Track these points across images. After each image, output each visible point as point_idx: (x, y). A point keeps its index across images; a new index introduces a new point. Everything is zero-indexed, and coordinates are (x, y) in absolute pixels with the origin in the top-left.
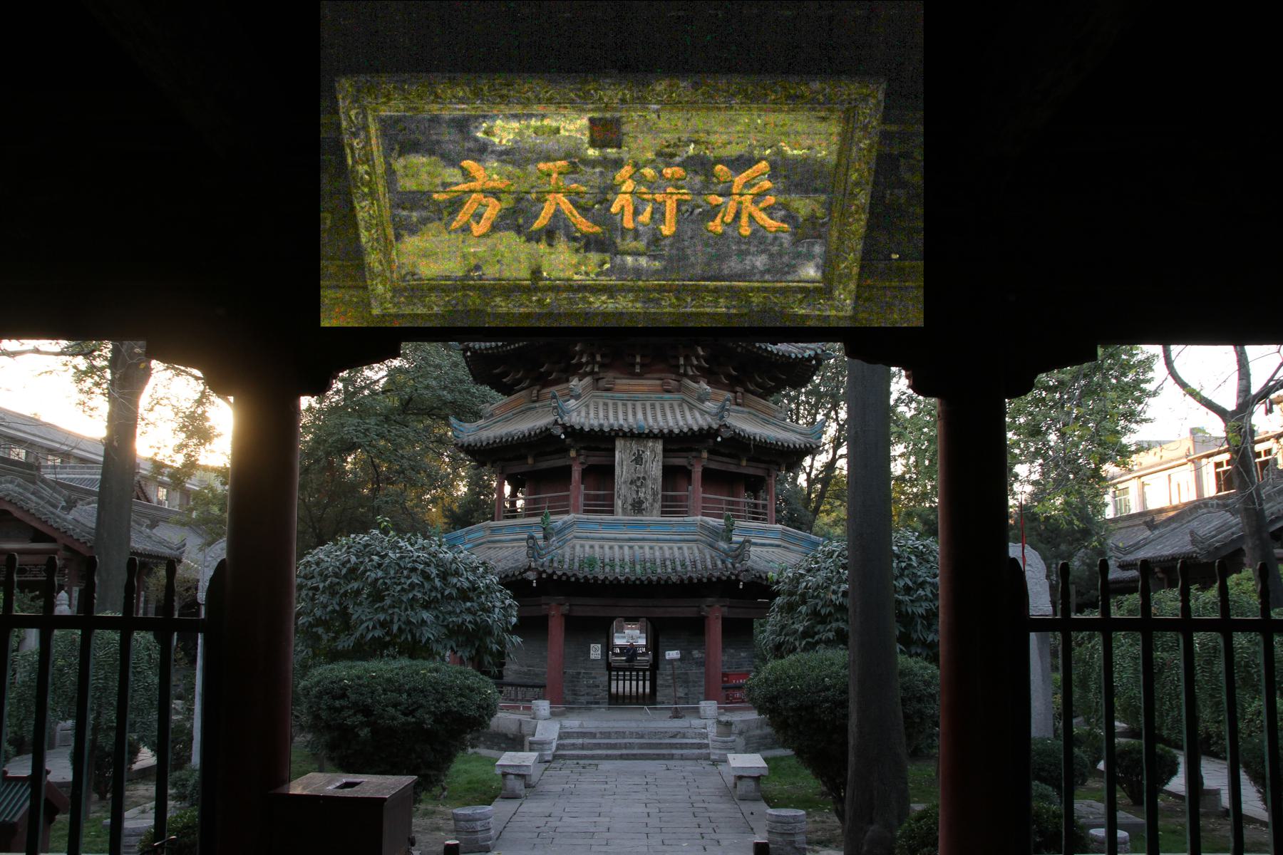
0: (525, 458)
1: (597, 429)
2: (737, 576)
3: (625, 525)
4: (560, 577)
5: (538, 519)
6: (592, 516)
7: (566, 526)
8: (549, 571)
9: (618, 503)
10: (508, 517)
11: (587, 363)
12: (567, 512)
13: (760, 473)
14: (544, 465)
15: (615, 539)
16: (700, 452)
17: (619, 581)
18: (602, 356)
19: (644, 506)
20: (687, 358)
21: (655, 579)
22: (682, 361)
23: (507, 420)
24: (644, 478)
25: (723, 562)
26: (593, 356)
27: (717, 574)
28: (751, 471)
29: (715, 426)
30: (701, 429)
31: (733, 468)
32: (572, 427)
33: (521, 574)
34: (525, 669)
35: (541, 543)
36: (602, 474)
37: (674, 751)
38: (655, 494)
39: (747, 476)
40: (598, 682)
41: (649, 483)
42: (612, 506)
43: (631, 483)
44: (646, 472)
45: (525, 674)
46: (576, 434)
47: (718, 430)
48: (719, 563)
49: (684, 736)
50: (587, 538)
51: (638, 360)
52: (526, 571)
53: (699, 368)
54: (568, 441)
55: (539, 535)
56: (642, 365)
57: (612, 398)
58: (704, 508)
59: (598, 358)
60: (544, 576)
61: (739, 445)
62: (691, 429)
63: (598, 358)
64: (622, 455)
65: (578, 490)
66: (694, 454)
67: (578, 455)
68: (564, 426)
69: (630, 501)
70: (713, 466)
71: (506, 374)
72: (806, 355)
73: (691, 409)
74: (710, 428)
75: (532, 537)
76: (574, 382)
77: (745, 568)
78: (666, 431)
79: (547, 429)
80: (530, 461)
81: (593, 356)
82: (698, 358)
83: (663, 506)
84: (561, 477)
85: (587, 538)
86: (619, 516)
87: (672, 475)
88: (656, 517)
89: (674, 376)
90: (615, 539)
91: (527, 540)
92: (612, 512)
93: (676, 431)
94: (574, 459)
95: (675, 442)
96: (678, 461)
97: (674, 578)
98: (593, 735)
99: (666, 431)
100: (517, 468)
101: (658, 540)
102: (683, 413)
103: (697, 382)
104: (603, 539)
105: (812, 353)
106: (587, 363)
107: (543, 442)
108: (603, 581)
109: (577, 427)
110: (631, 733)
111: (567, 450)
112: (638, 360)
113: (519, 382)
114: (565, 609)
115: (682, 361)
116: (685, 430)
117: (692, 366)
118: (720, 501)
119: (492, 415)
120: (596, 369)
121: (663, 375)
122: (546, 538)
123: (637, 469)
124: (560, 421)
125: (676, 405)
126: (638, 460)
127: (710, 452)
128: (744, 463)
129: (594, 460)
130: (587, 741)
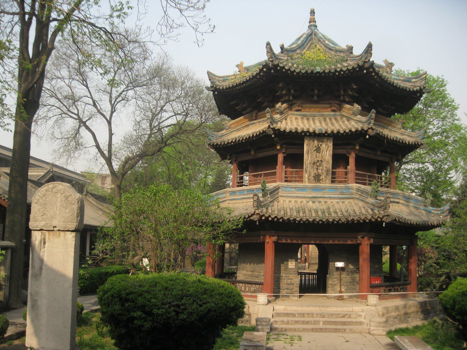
0: (250, 151)
1: (294, 131)
2: (381, 219)
3: (310, 188)
4: (273, 219)
5: (259, 186)
6: (289, 184)
7: (277, 189)
8: (267, 215)
9: (306, 176)
10: (238, 186)
11: (286, 95)
12: (275, 181)
13: (387, 160)
14: (260, 155)
15: (305, 197)
16: (355, 145)
17: (309, 221)
18: (295, 91)
19: (321, 178)
20: (345, 91)
21: (331, 220)
22: (342, 93)
23: (238, 130)
24: (321, 161)
25: (372, 210)
26: (289, 90)
27: (369, 217)
28: (382, 158)
29: (366, 129)
30: (357, 131)
31: (372, 156)
32: (279, 130)
33: (249, 217)
34: (250, 273)
35: (261, 199)
36: (296, 160)
37: (345, 327)
38: (328, 171)
39: (379, 161)
40: (293, 282)
41: (324, 164)
42: (302, 177)
43: (314, 164)
44: (322, 157)
45: (249, 276)
46: (281, 135)
47: (367, 131)
48: (370, 211)
49: (350, 317)
50: (288, 197)
51: (316, 92)
52: (252, 215)
53: (352, 97)
54: (276, 139)
55: (260, 195)
56: (318, 96)
57: (300, 115)
58: (356, 179)
59: (292, 92)
60: (263, 218)
61: (379, 141)
62: (350, 131)
63: (292, 92)
64: (308, 146)
65: (280, 168)
66: (351, 147)
67: (281, 148)
68: (273, 129)
69: (313, 174)
70: (361, 154)
71: (237, 105)
72: (415, 89)
73: (348, 120)
74: (362, 129)
75: (256, 195)
76: (279, 104)
77: (386, 214)
78: (335, 132)
79: (264, 132)
80: (252, 153)
81: (289, 90)
82: (352, 90)
83: (332, 178)
84: (271, 162)
85: (288, 197)
86: (306, 184)
87: (339, 160)
88: (328, 184)
89: (337, 102)
90: (305, 197)
91: (253, 198)
92: (302, 181)
93: (342, 132)
94: (279, 150)
95: (341, 141)
96: (340, 151)
97: (343, 220)
98: (294, 315)
99: (335, 132)
100: (244, 158)
101: (330, 198)
102: (343, 122)
103: (353, 105)
104: (297, 197)
105: (418, 88)
106: (286, 95)
107: (262, 141)
108: (299, 221)
109: (282, 130)
110: (317, 314)
111: (275, 145)
112: (316, 92)
113: (245, 109)
114: (274, 238)
115: (342, 93)
116: (347, 131)
117: (348, 95)
118: (365, 176)
119: (230, 128)
120: (291, 98)
121: (331, 101)
122: (264, 196)
123: (318, 156)
124: (271, 126)
125: (339, 118)
126: (318, 150)
127: (361, 146)
128: (379, 153)
129: (291, 151)
130: (290, 319)
